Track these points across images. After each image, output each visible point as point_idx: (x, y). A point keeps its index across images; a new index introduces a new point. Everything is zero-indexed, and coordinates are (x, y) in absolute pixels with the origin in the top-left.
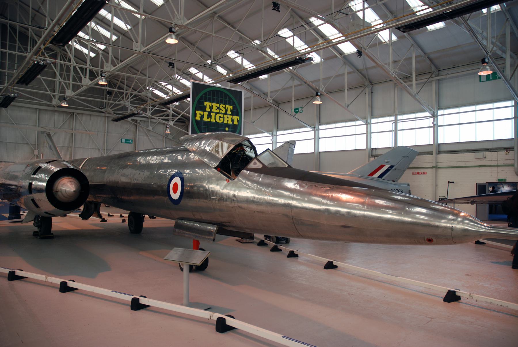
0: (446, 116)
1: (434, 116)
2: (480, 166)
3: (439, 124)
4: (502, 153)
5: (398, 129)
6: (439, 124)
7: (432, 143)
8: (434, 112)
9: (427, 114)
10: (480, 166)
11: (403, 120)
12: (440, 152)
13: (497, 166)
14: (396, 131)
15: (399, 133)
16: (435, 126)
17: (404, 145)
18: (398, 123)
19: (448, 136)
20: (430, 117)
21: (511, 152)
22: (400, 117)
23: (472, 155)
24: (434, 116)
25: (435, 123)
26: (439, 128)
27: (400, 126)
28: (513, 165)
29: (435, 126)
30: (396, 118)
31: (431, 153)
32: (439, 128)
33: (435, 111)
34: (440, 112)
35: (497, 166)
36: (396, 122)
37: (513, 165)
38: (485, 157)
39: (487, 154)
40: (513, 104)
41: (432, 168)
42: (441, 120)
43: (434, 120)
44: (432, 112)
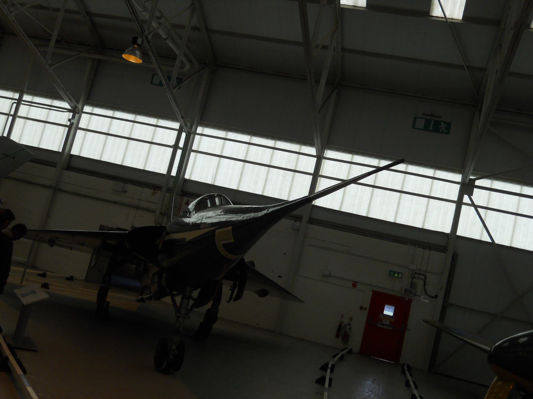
0: (94, 118)
1: (76, 112)
2: (115, 203)
3: (80, 126)
4: (149, 191)
5: (19, 114)
6: (80, 126)
7: (61, 151)
8: (76, 107)
9: (66, 105)
10: (115, 203)
11: (31, 104)
12: (69, 168)
13: (137, 208)
14: (15, 116)
15: (18, 120)
16: (72, 128)
17: (21, 143)
18: (22, 106)
19: (87, 147)
20: (69, 111)
21: (159, 193)
22: (26, 97)
23: (110, 183)
24: (76, 112)
25: (75, 121)
26: (78, 131)
27: (23, 110)
28: (153, 212)
29: (72, 128)
30: (21, 97)
31: (53, 165)
32: (78, 131)
33: (80, 106)
34: (87, 109)
35: (137, 208)
36: (19, 102)
37: (153, 212)
38: (126, 192)
39: (130, 187)
40: (178, 128)
41: (50, 187)
42: (84, 121)
43: (73, 117)
44: (73, 105)
